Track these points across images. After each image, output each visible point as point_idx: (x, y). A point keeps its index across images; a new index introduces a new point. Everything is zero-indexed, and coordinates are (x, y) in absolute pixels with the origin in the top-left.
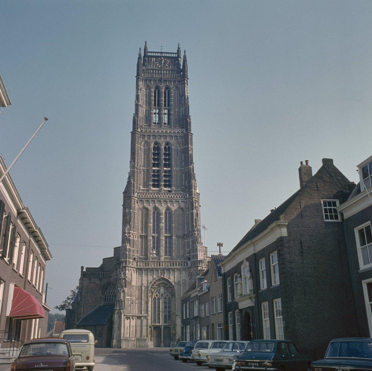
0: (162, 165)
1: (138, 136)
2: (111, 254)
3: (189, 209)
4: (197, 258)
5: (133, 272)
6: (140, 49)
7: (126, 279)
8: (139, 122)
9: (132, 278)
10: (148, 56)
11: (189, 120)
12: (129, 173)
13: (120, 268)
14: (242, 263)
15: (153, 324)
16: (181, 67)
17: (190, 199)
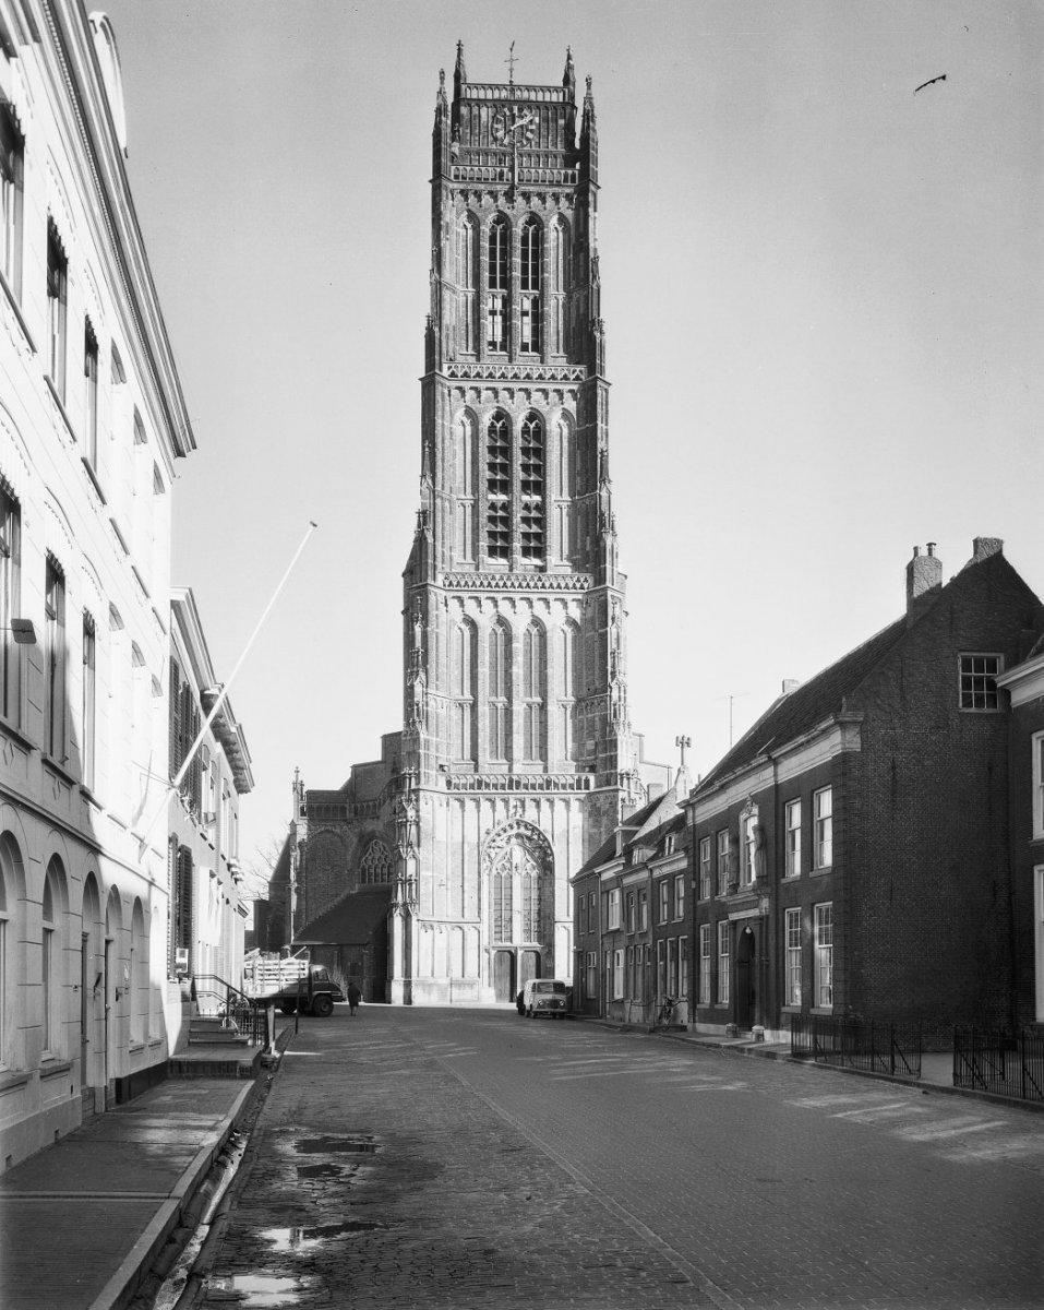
0: (517, 486)
1: (443, 394)
2: (375, 755)
3: (593, 624)
5: (437, 804)
6: (442, 72)
8: (444, 345)
9: (437, 823)
10: (469, 102)
11: (597, 335)
12: (419, 513)
13: (402, 792)
14: (740, 806)
15: (494, 944)
16: (577, 145)
17: (598, 594)
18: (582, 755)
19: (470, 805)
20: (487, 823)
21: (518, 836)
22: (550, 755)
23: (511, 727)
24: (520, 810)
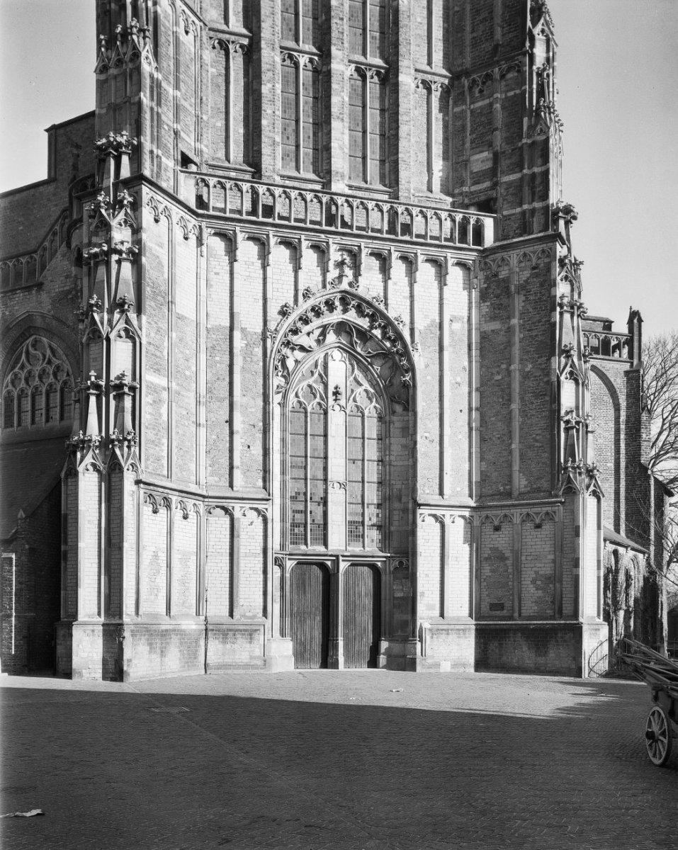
4: (545, 196)
7: (144, 259)
15: (290, 548)
18: (462, 184)
19: (247, 250)
20: (281, 293)
21: (342, 328)
22: (403, 175)
23: (328, 107)
24: (349, 272)
